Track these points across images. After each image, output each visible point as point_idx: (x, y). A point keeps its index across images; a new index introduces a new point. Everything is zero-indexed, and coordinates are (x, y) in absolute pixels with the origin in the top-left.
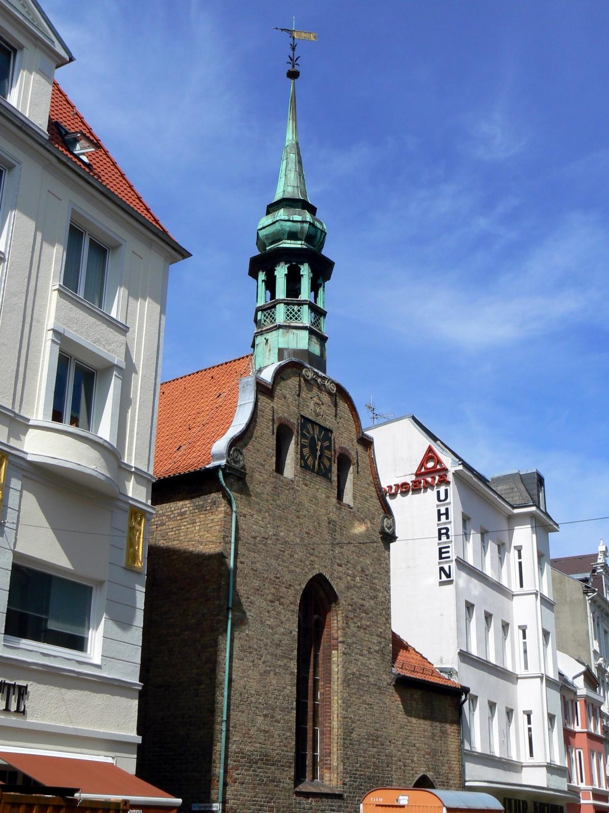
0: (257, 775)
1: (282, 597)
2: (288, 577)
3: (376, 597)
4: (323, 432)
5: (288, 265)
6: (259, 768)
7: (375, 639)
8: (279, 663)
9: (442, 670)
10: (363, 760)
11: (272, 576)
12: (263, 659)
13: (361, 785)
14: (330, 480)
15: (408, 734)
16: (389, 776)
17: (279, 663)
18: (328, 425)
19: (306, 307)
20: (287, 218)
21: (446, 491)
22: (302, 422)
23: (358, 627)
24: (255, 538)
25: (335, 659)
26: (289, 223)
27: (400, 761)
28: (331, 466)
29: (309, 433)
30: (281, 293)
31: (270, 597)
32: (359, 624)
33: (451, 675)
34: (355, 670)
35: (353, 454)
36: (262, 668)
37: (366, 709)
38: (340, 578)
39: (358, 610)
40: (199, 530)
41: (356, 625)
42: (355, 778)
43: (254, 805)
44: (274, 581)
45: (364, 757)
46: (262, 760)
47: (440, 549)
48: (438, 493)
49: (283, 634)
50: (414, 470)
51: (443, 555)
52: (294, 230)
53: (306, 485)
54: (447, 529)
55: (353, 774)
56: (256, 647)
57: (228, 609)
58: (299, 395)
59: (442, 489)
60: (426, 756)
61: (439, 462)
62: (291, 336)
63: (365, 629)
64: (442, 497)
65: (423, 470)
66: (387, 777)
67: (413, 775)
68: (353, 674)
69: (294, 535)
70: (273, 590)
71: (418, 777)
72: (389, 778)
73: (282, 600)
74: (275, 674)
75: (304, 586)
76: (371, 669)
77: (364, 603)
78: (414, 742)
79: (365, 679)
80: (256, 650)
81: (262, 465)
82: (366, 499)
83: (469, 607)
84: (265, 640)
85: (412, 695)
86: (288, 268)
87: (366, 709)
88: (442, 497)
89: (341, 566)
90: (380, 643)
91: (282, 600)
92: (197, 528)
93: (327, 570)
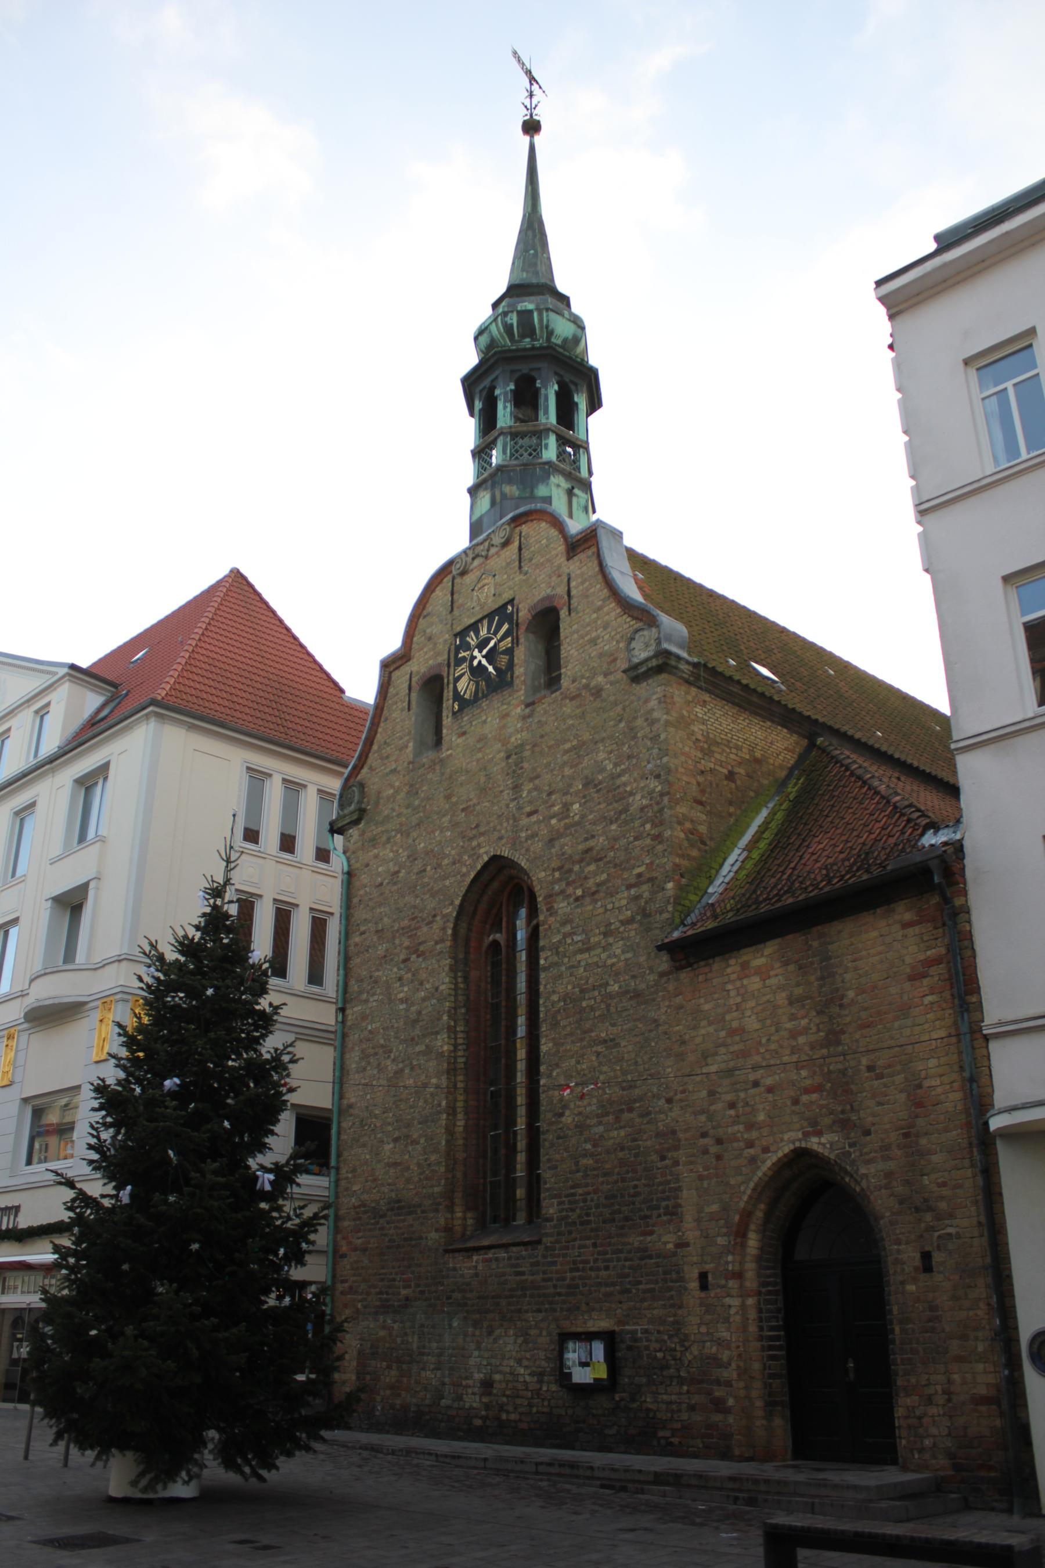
0: (386, 1235)
1: (420, 944)
4: (497, 618)
6: (388, 1223)
8: (418, 1049)
10: (591, 1162)
12: (392, 1056)
13: (588, 1215)
15: (732, 1064)
16: (669, 1178)
17: (418, 1049)
22: (458, 643)
23: (577, 899)
27: (704, 1135)
31: (402, 957)
32: (579, 892)
34: (570, 987)
36: (392, 1067)
37: (598, 1054)
39: (576, 868)
41: (572, 900)
42: (570, 1202)
43: (382, 1280)
44: (410, 926)
45: (592, 1155)
46: (392, 1209)
49: (424, 999)
55: (567, 1196)
56: (382, 1042)
60: (805, 1098)
63: (594, 894)
66: (660, 1184)
67: (753, 1160)
72: (668, 1182)
73: (421, 948)
74: (412, 1069)
76: (613, 965)
77: (591, 843)
78: (752, 1077)
79: (596, 993)
80: (382, 1046)
84: (396, 1025)
85: (745, 966)
87: (598, 1054)
89: (535, 812)
91: (421, 948)
93: (504, 841)
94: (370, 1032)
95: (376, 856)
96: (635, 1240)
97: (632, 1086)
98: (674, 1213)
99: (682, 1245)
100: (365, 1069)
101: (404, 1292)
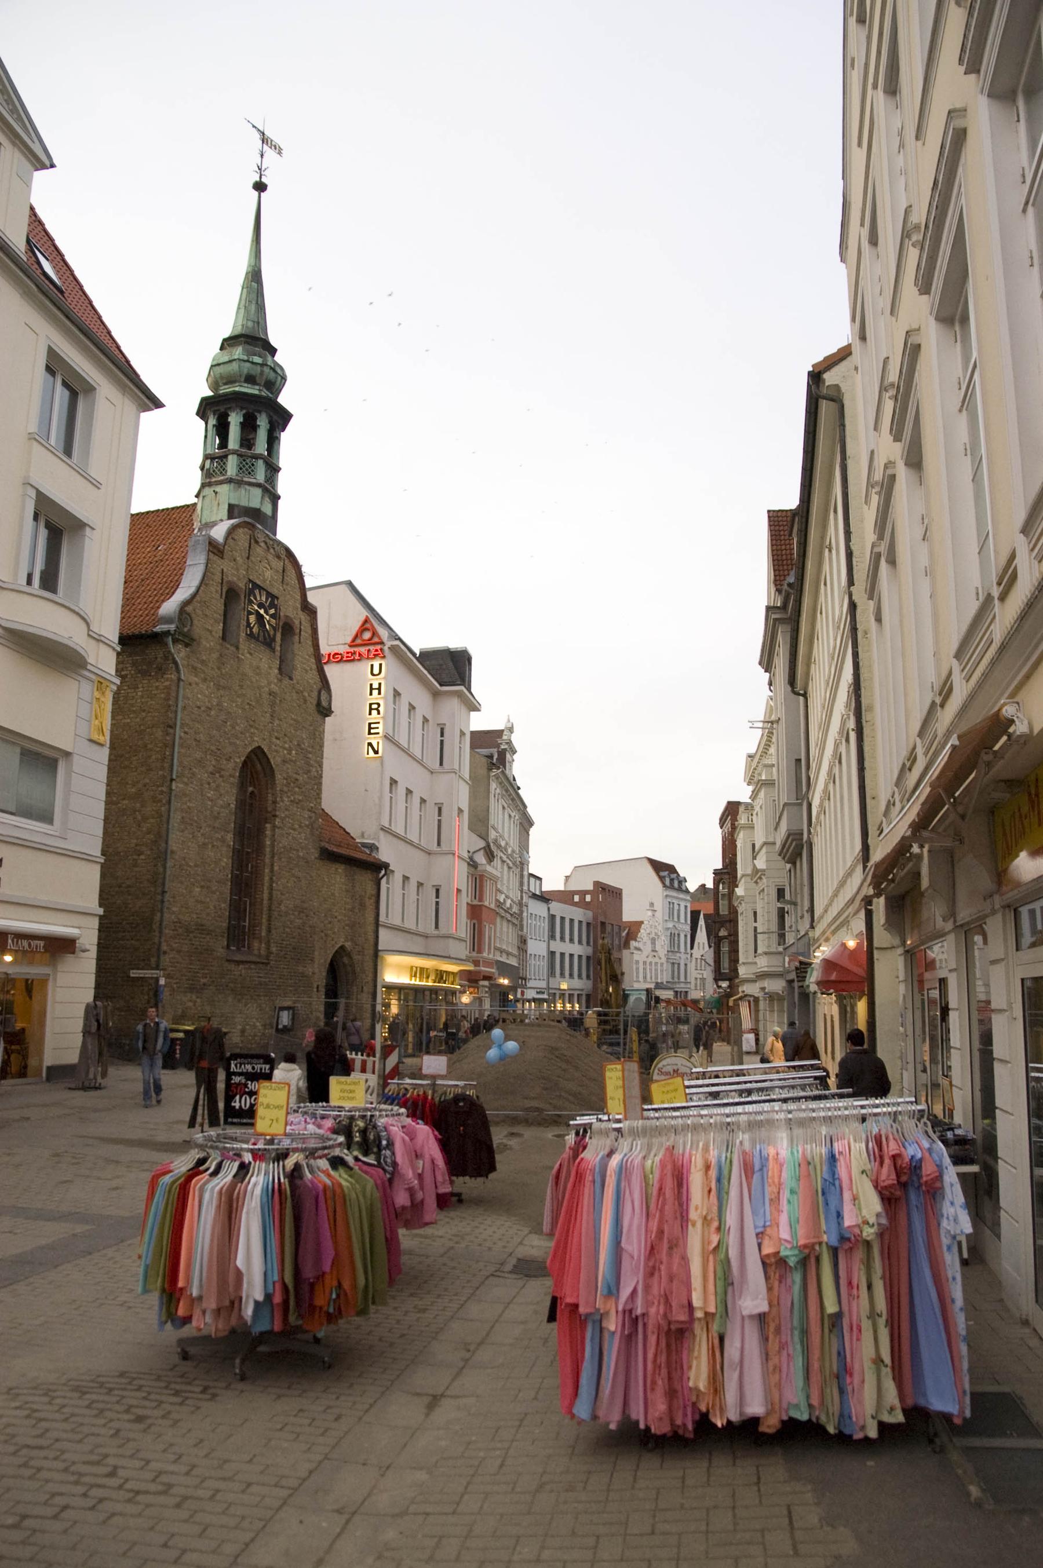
2: (229, 749)
3: (309, 771)
5: (244, 411)
7: (306, 814)
9: (364, 845)
11: (213, 748)
14: (273, 650)
18: (275, 592)
19: (260, 462)
20: (245, 358)
21: (381, 665)
24: (199, 707)
25: (268, 832)
26: (248, 365)
28: (275, 635)
29: (256, 599)
30: (233, 443)
31: (211, 769)
33: (372, 851)
35: (297, 622)
36: (201, 840)
38: (277, 751)
40: (142, 697)
47: (370, 724)
48: (372, 666)
49: (222, 807)
50: (349, 639)
51: (372, 731)
52: (253, 373)
53: (251, 654)
54: (379, 705)
57: (172, 780)
58: (248, 558)
59: (376, 664)
61: (375, 633)
62: (243, 491)
64: (376, 671)
65: (358, 641)
68: (284, 847)
69: (237, 706)
70: (213, 763)
71: (338, 946)
75: (243, 759)
77: (298, 777)
81: (211, 632)
82: (307, 671)
83: (393, 782)
86: (244, 416)
88: (376, 671)
90: (310, 817)
92: (140, 694)
94: (189, 807)
95: (197, 684)
96: (301, 969)
97: (303, 902)
98: (312, 960)
99: (313, 973)
100: (183, 831)
101: (203, 981)
